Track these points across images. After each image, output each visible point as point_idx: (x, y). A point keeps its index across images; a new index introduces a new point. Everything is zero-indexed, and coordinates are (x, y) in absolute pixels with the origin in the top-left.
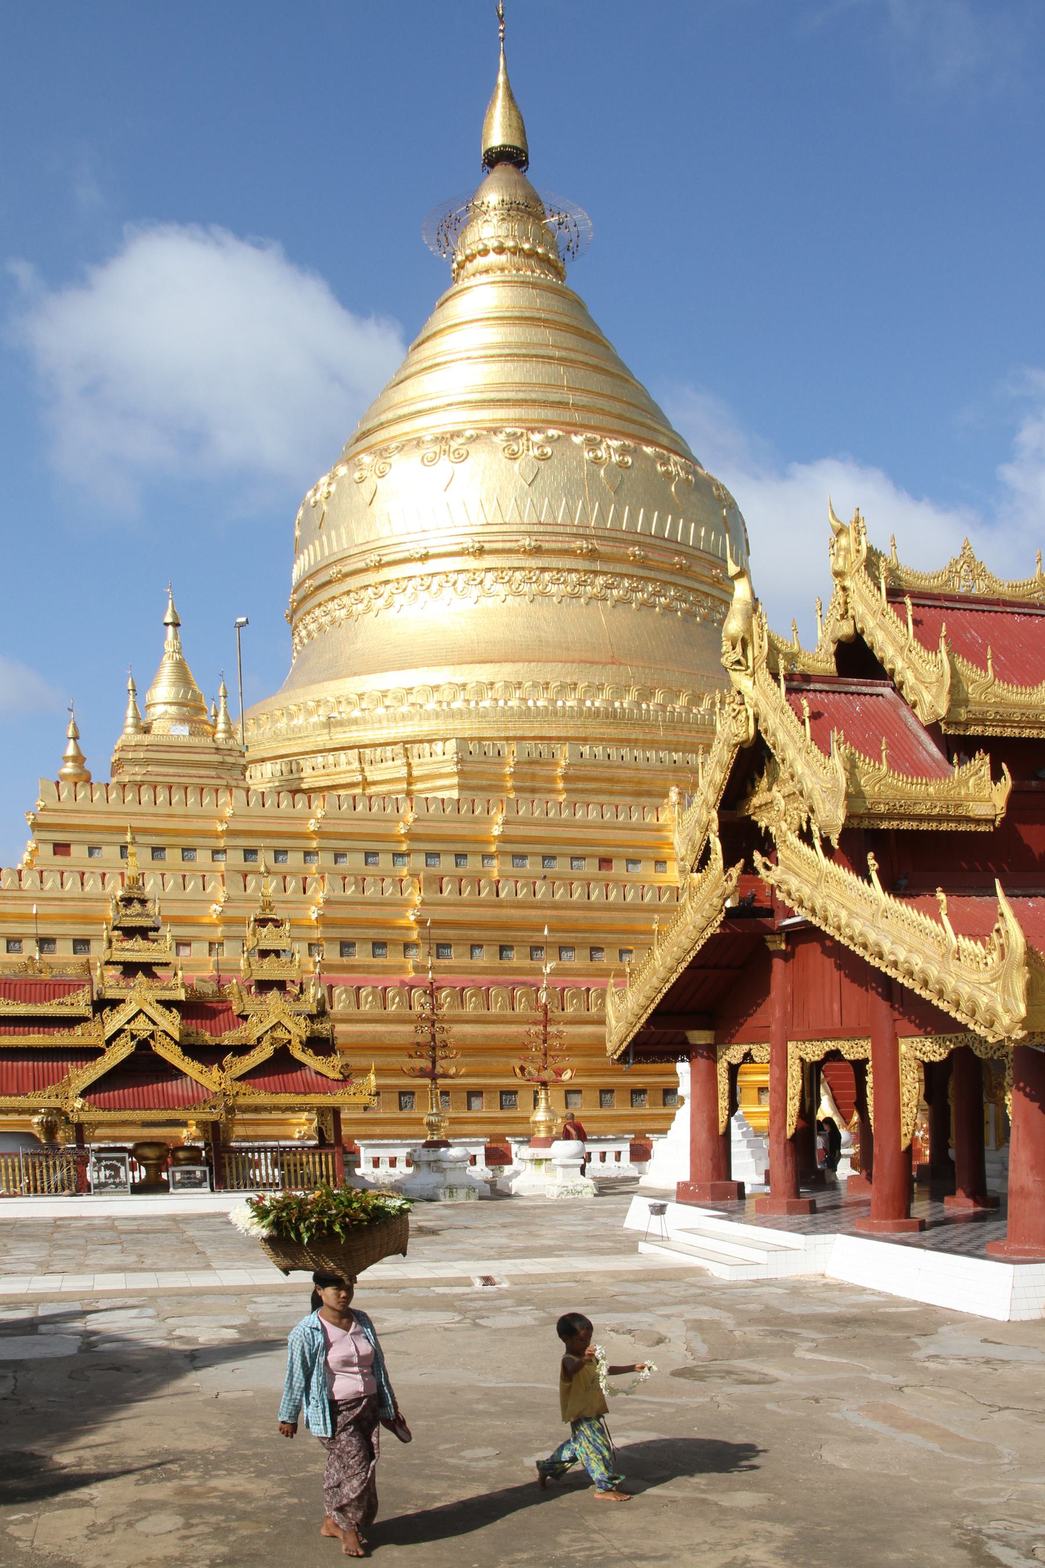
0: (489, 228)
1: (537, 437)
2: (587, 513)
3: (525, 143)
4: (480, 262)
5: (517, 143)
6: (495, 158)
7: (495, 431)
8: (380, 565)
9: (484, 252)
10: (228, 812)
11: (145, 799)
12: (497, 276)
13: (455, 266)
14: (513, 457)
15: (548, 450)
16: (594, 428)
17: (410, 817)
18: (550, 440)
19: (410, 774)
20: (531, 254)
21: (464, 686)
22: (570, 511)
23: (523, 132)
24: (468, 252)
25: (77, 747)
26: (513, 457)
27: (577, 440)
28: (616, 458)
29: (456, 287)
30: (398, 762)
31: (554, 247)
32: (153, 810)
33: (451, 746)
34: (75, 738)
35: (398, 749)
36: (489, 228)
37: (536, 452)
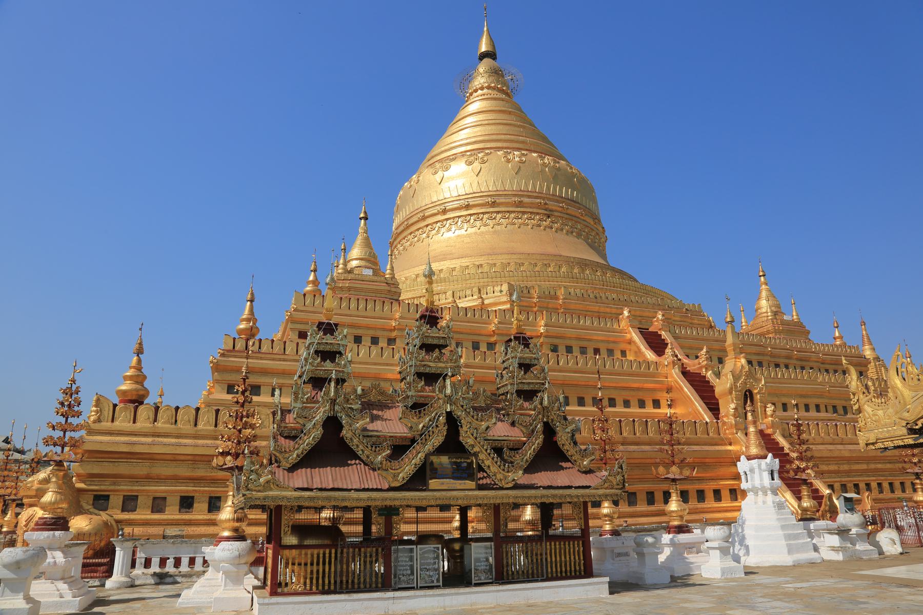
10: (397, 315)
11: (352, 306)
14: (508, 161)
17: (496, 321)
18: (523, 155)
19: (483, 303)
20: (501, 91)
21: (495, 264)
22: (534, 186)
23: (494, 46)
25: (315, 276)
26: (508, 161)
30: (475, 297)
31: (508, 87)
32: (356, 313)
33: (505, 287)
34: (315, 271)
35: (475, 290)
36: (480, 80)
37: (517, 159)
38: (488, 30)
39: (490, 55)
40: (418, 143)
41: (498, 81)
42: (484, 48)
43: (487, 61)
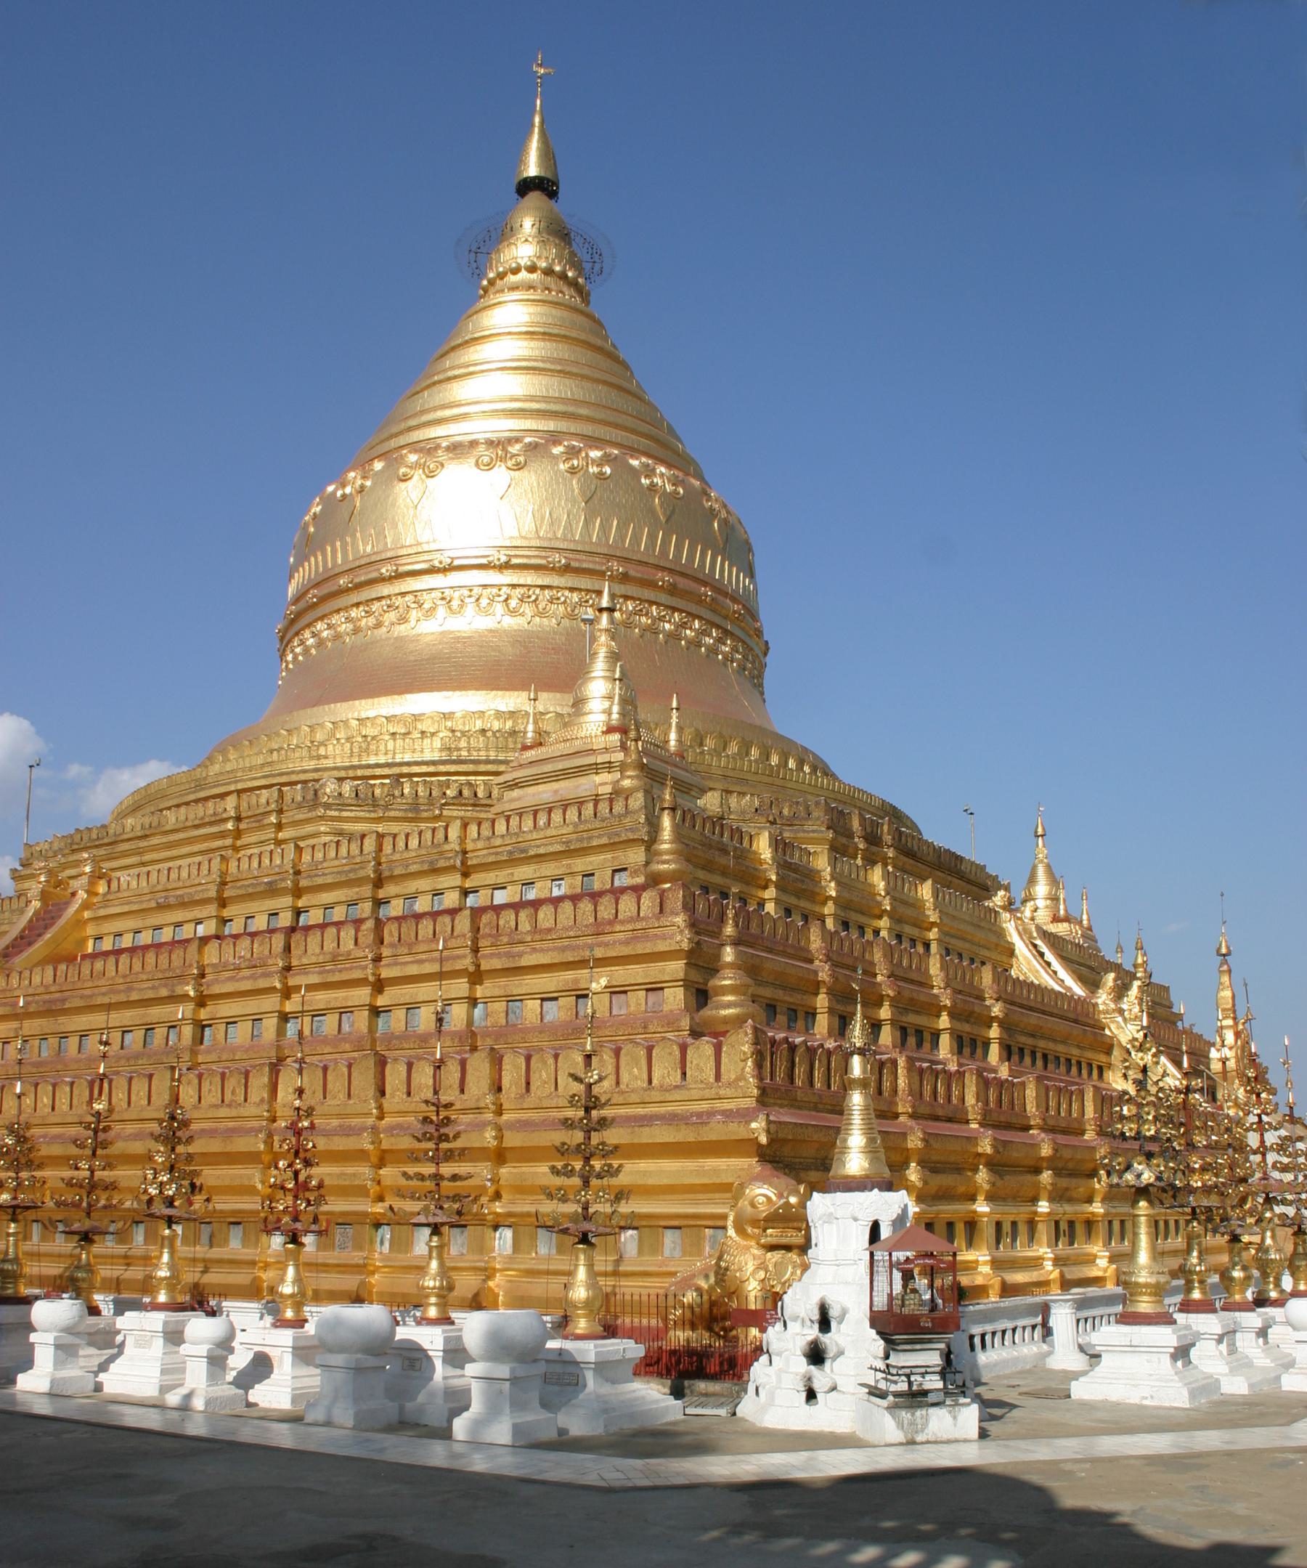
0: (525, 248)
1: (595, 454)
2: (642, 541)
3: (557, 175)
4: (512, 278)
5: (549, 175)
6: (526, 187)
7: (557, 442)
8: (400, 576)
9: (516, 271)
12: (530, 295)
13: (485, 282)
15: (607, 470)
16: (649, 456)
24: (501, 269)
27: (635, 463)
28: (669, 488)
29: (483, 302)
36: (525, 248)
38: (542, 122)
39: (545, 186)
40: (374, 390)
41: (560, 257)
42: (532, 169)
43: (535, 197)
